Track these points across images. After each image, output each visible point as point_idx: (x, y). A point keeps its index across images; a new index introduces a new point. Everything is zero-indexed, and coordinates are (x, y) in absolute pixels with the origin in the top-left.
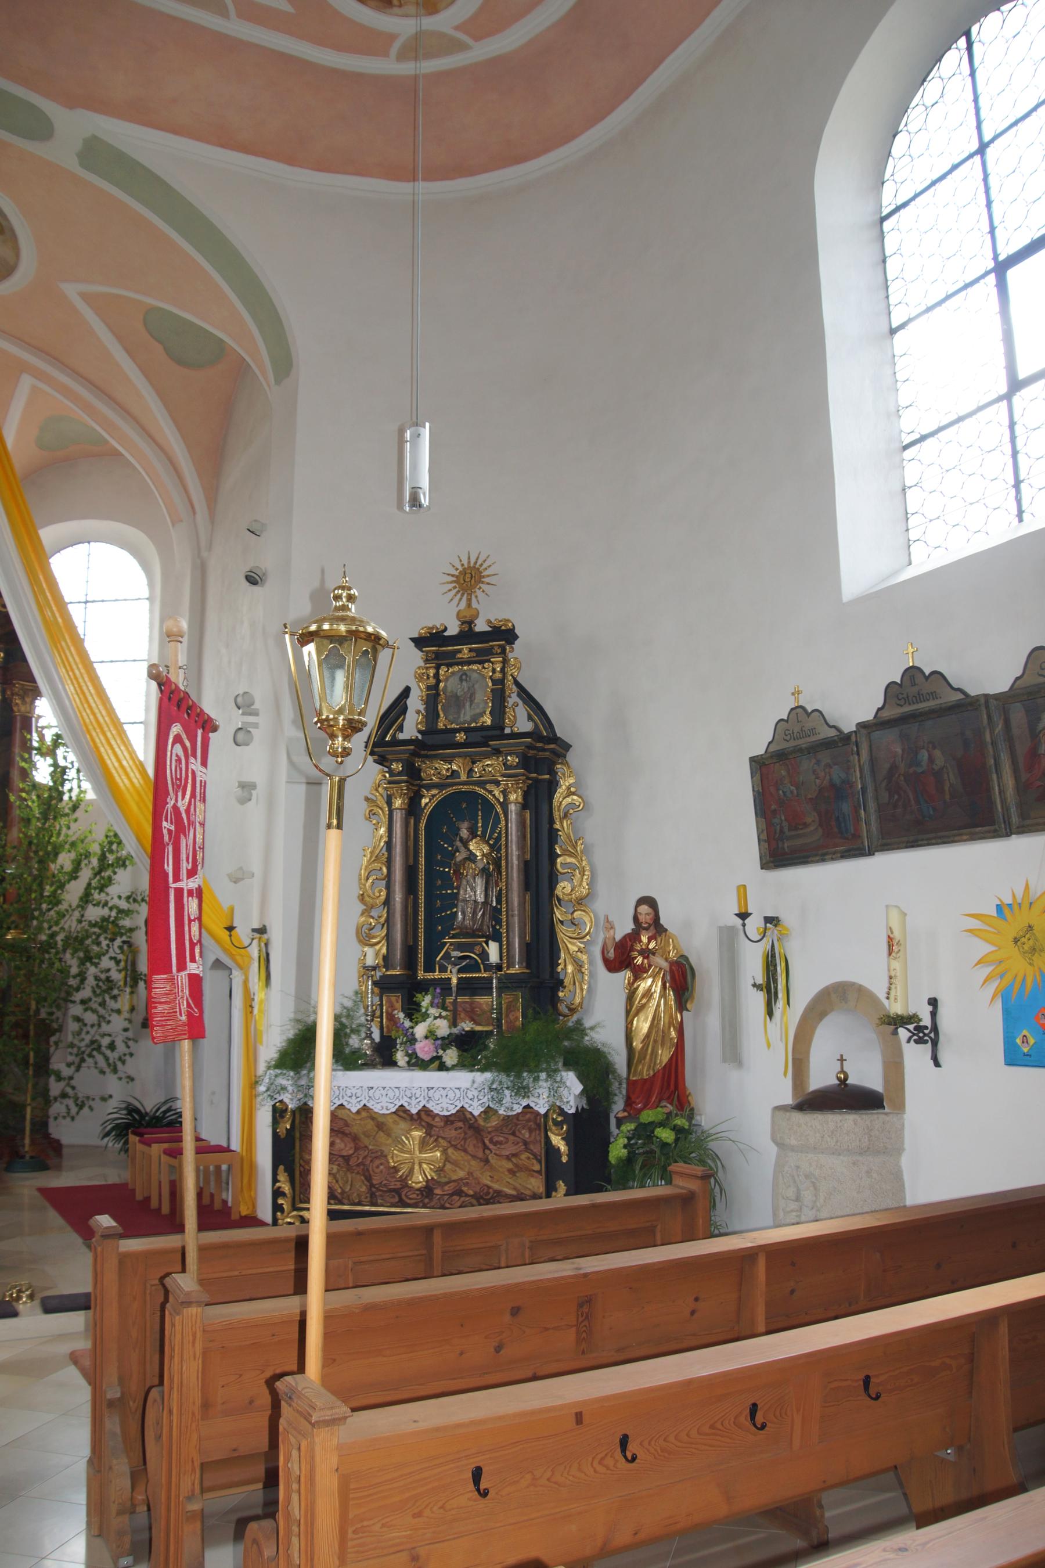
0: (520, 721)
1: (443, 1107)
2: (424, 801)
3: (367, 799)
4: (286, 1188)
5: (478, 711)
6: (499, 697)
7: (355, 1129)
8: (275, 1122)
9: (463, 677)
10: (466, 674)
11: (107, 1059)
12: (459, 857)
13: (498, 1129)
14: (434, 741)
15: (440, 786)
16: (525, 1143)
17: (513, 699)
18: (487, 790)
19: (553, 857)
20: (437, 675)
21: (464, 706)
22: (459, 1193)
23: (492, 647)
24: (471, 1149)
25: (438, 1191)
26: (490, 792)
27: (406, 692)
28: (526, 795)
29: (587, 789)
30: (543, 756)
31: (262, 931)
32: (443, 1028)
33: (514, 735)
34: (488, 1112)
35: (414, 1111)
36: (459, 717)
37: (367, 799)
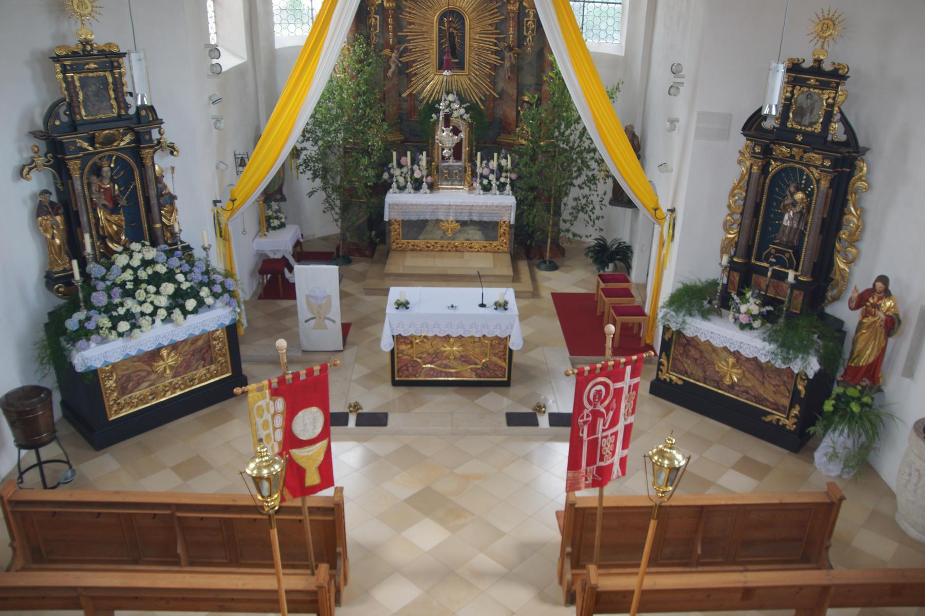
1: (747, 353)
3: (740, 152)
4: (665, 363)
5: (814, 120)
6: (828, 117)
7: (702, 348)
8: (664, 333)
9: (809, 96)
11: (590, 217)
12: (788, 201)
14: (783, 134)
15: (782, 161)
16: (784, 382)
17: (837, 117)
20: (792, 92)
22: (747, 393)
23: (831, 82)
24: (757, 375)
25: (737, 388)
29: (876, 171)
31: (672, 211)
32: (755, 310)
35: (732, 350)
37: (740, 152)
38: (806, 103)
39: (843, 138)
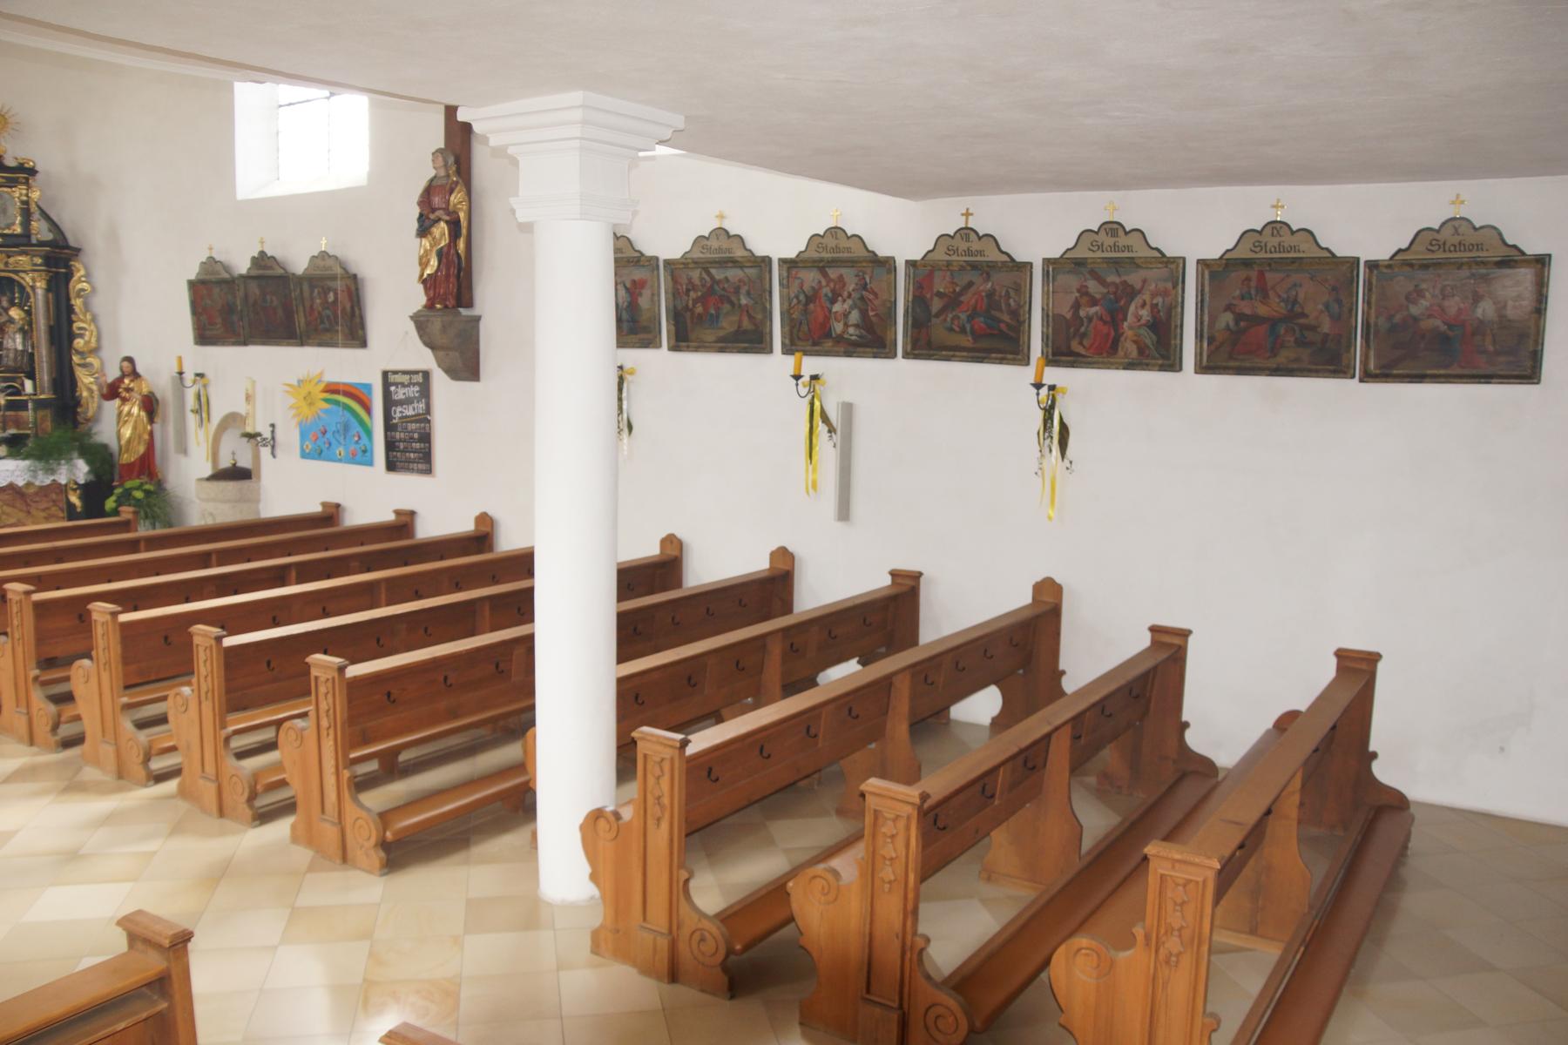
0: (40, 230)
6: (26, 214)
13: (36, 494)
17: (37, 215)
19: (71, 322)
28: (49, 282)
30: (61, 258)
33: (41, 244)
34: (29, 484)
39: (49, 236)
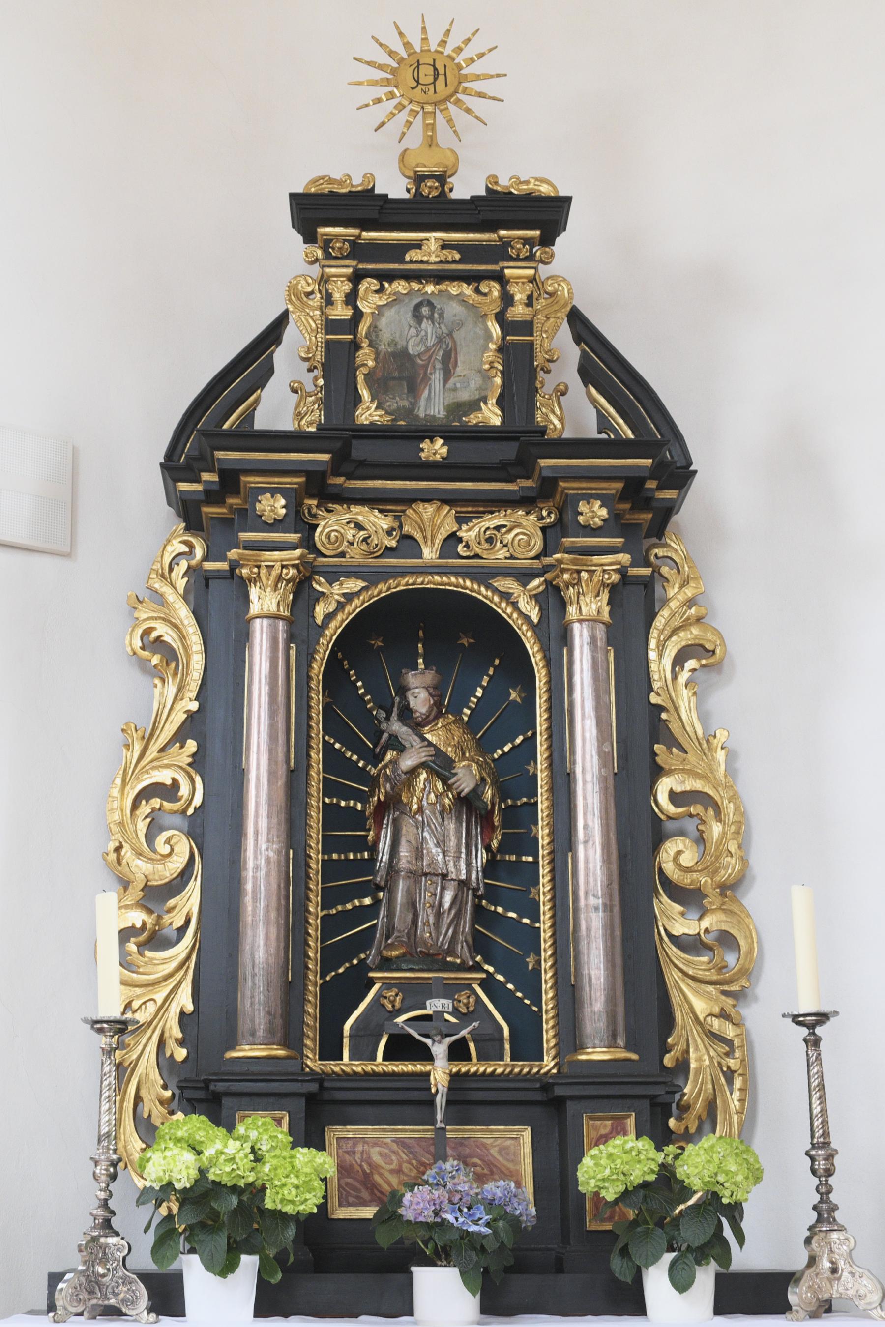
2: (320, 611)
5: (464, 396)
10: (430, 304)
14: (347, 459)
18: (495, 590)
21: (426, 379)
23: (506, 244)
26: (506, 596)
27: (273, 334)
36: (414, 405)
38: (418, 339)
